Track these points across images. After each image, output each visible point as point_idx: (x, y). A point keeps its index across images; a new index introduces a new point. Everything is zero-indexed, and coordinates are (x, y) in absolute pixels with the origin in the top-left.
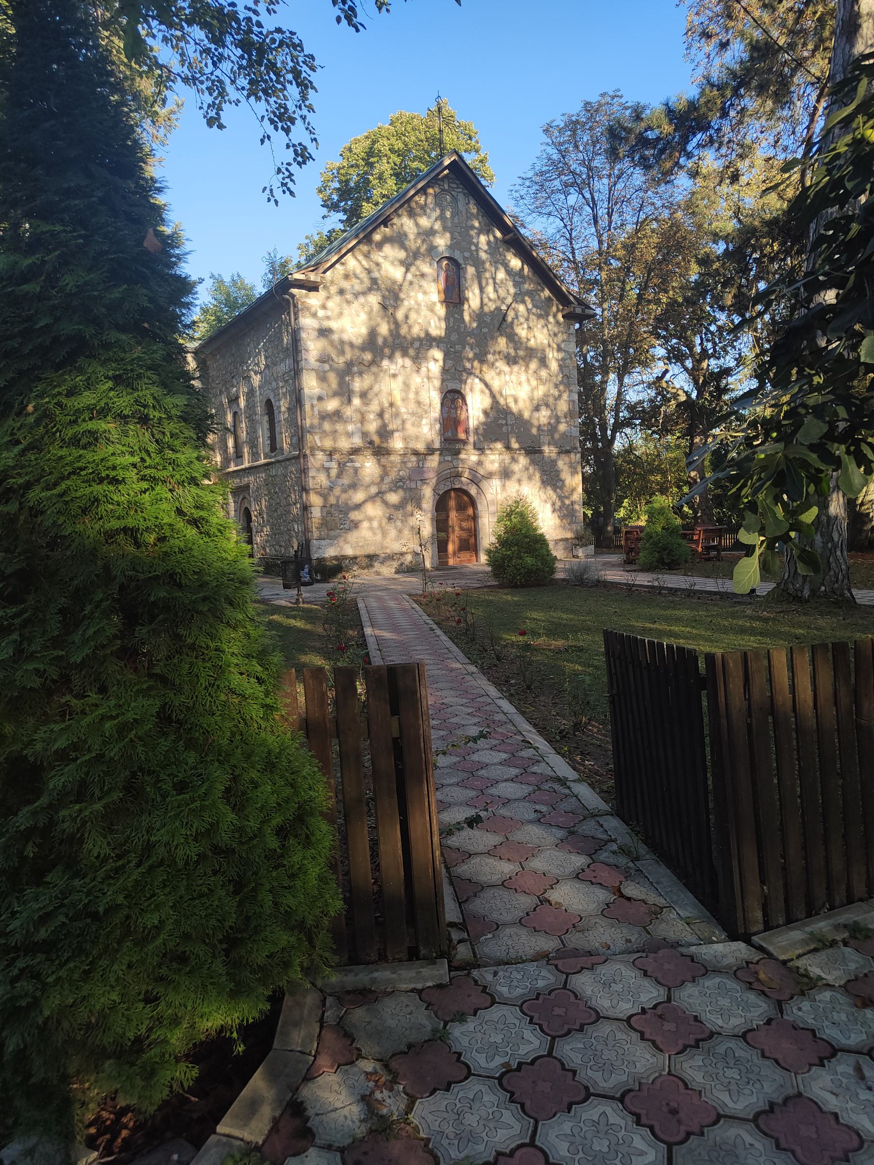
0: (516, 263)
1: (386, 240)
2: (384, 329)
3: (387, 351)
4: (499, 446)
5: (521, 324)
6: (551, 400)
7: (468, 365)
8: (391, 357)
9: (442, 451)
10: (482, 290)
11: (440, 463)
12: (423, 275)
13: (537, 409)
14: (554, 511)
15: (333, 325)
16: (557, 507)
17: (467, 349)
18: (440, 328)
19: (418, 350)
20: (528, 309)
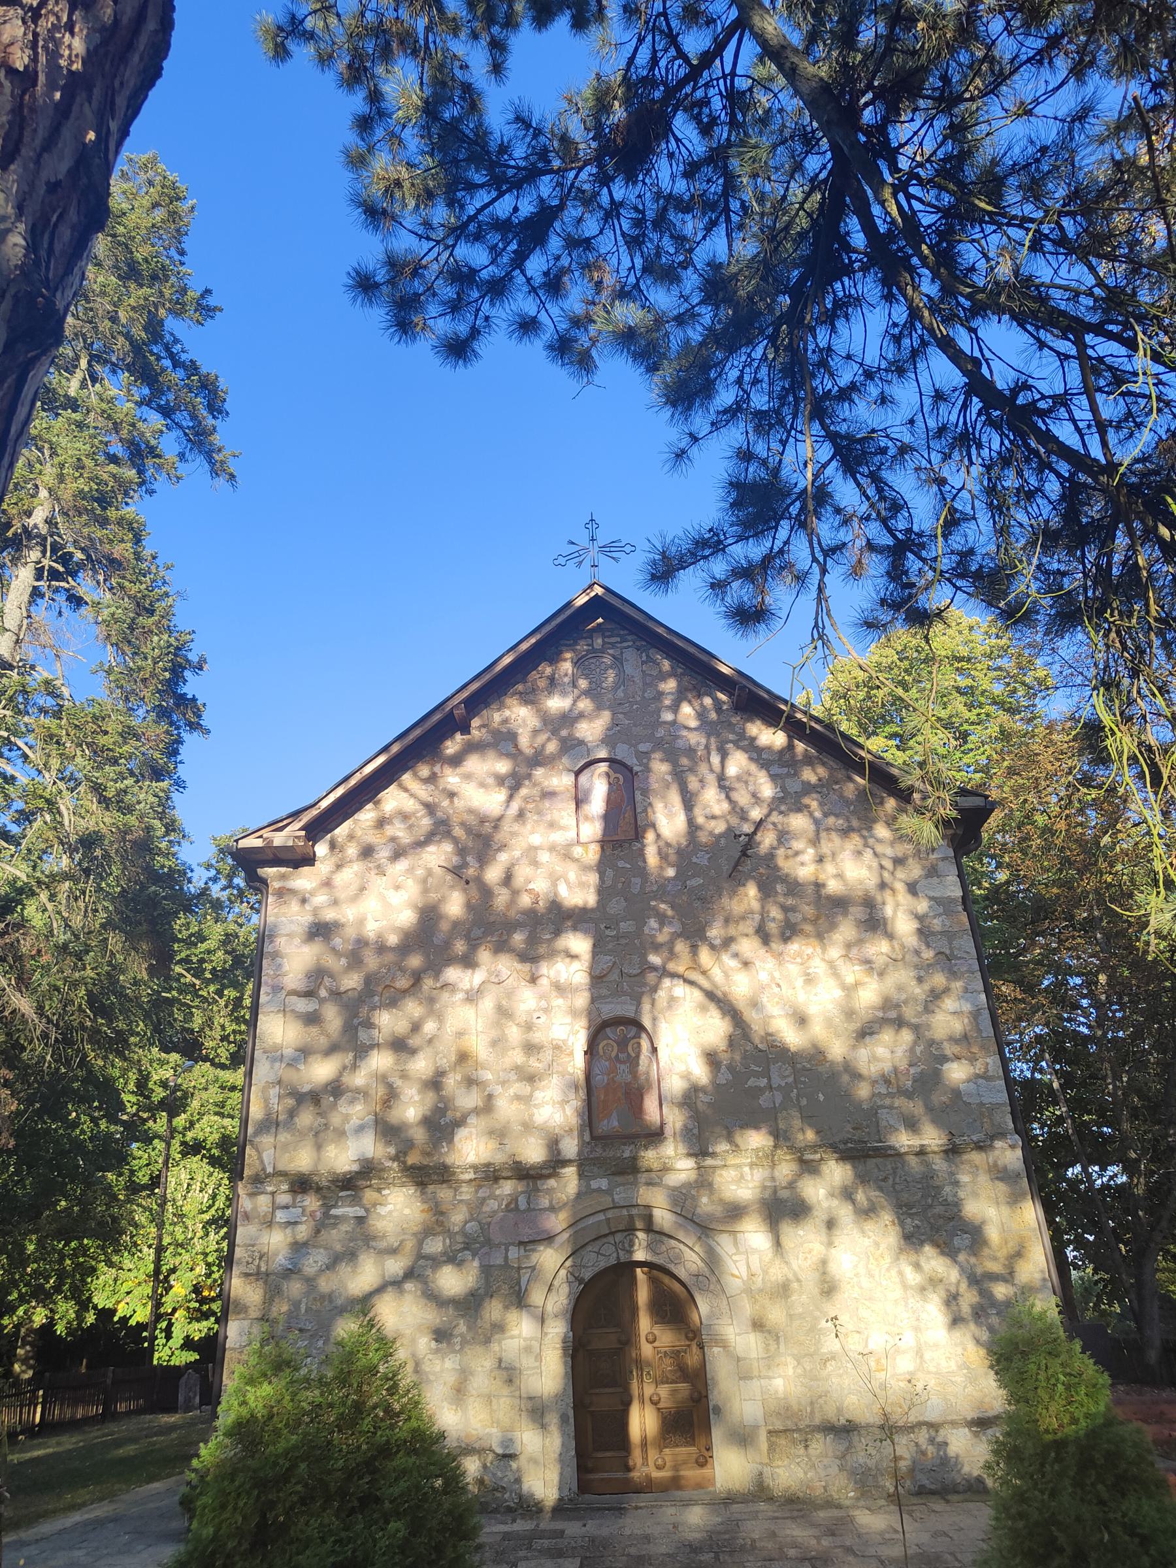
0: (772, 738)
1: (472, 748)
2: (455, 906)
3: (460, 947)
4: (756, 1140)
5: (797, 854)
6: (909, 1013)
7: (655, 959)
8: (468, 962)
9: (586, 1164)
10: (689, 802)
11: (579, 1195)
12: (548, 795)
13: (865, 1033)
14: (956, 1321)
15: (348, 914)
16: (966, 1309)
17: (653, 923)
18: (582, 885)
19: (533, 940)
20: (817, 822)
